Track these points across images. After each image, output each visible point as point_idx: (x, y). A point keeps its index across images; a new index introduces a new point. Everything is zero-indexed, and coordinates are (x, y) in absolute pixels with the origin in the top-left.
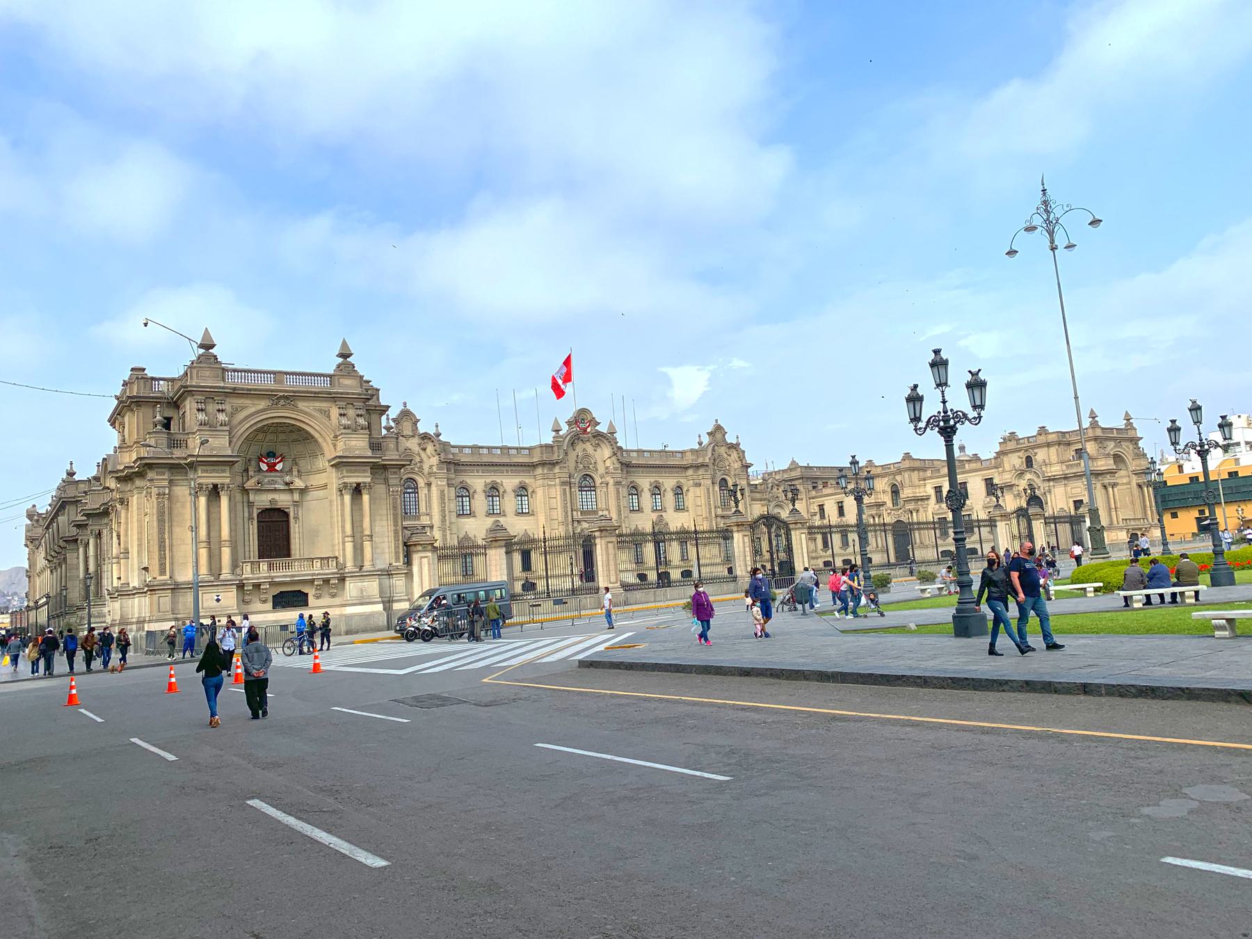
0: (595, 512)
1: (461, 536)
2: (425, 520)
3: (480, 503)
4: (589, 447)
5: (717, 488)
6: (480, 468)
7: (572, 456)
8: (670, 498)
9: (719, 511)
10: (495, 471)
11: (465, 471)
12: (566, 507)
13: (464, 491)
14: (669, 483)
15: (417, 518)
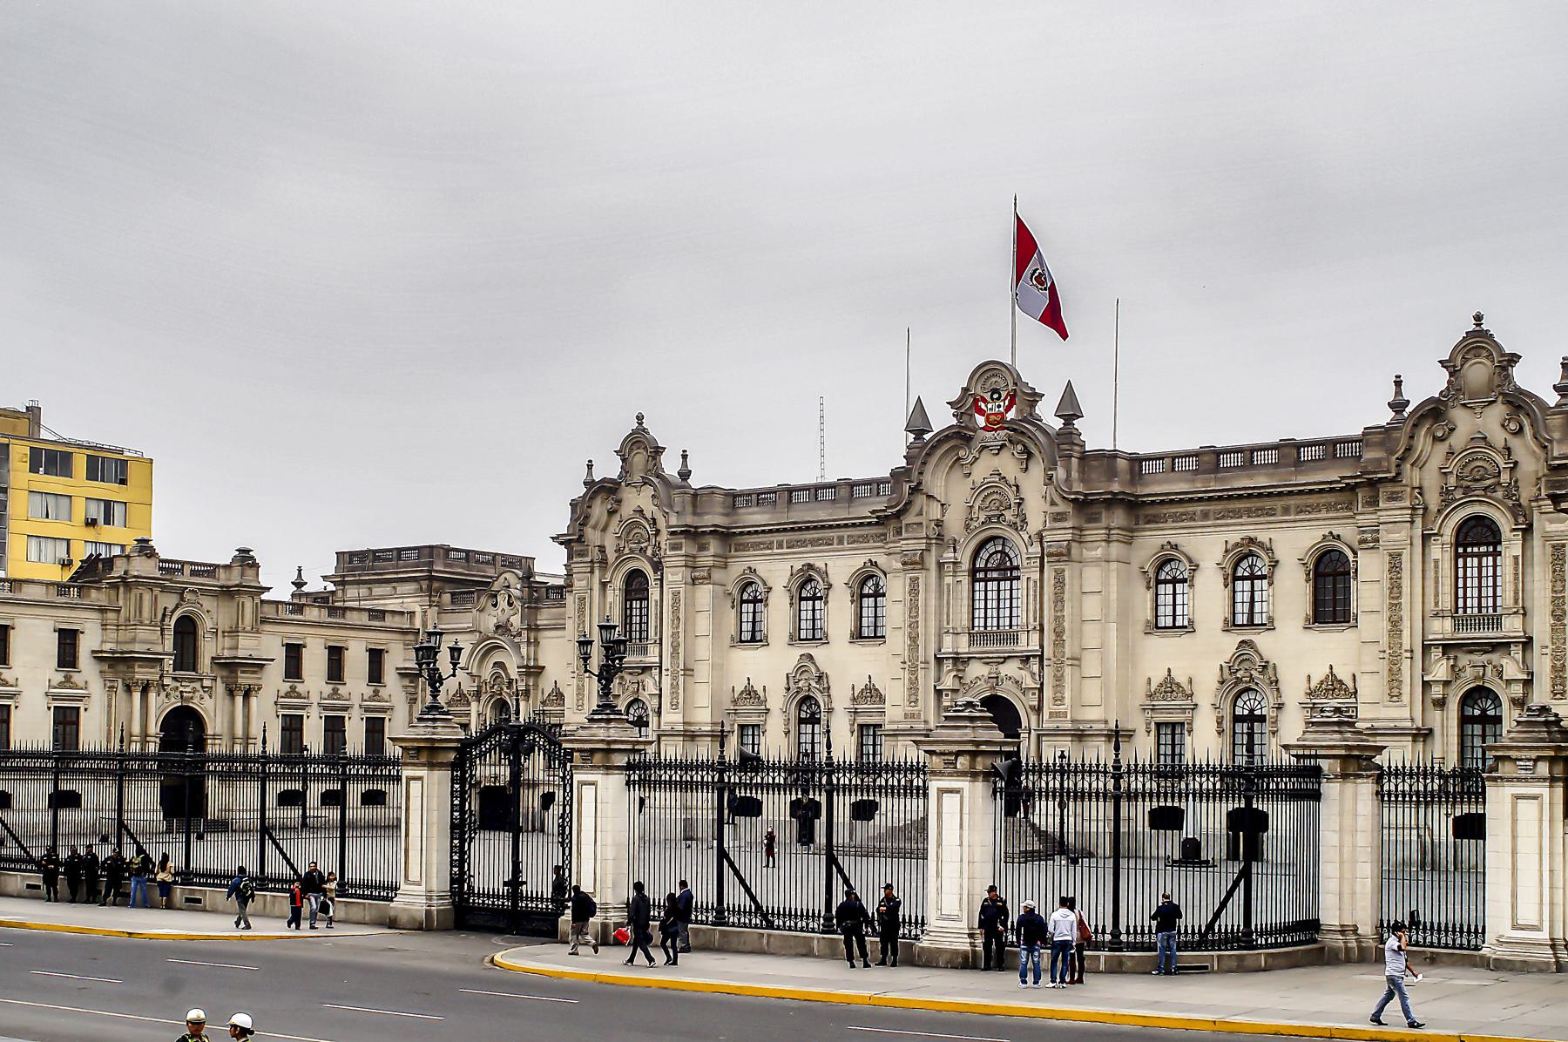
0: (1016, 640)
1: (739, 689)
2: (652, 658)
3: (778, 615)
4: (1008, 464)
5: (1441, 552)
6: (784, 537)
7: (952, 495)
8: (1290, 592)
9: (1442, 628)
10: (813, 542)
11: (756, 546)
12: (913, 625)
13: (750, 595)
14: (1293, 542)
15: (644, 651)
